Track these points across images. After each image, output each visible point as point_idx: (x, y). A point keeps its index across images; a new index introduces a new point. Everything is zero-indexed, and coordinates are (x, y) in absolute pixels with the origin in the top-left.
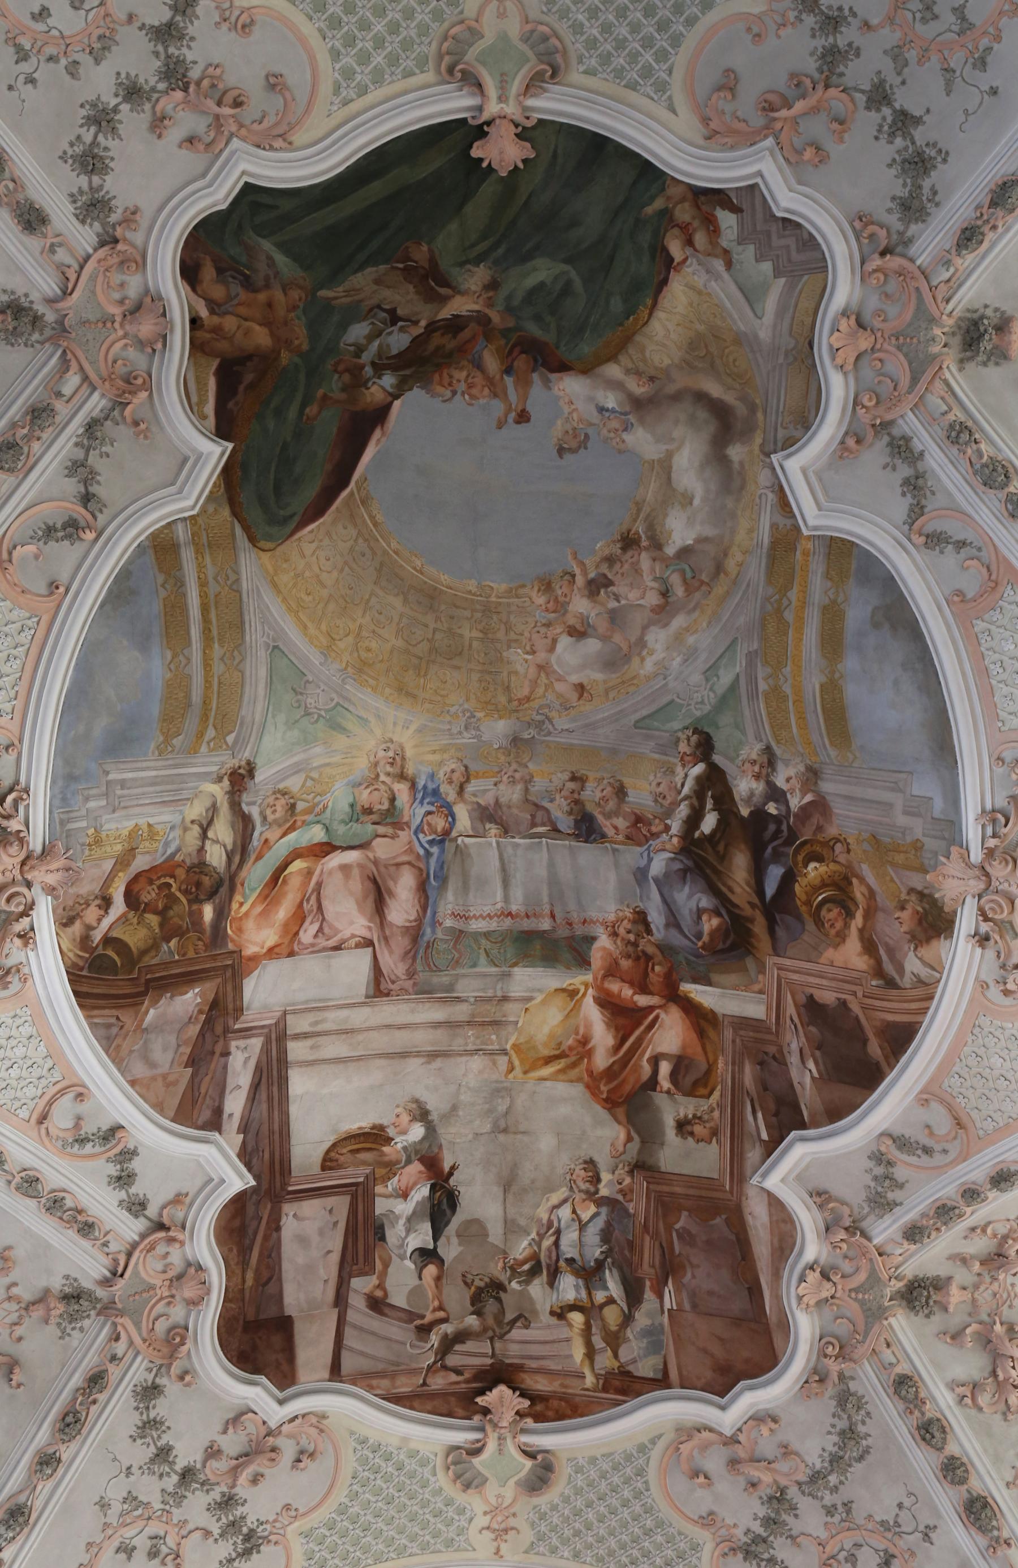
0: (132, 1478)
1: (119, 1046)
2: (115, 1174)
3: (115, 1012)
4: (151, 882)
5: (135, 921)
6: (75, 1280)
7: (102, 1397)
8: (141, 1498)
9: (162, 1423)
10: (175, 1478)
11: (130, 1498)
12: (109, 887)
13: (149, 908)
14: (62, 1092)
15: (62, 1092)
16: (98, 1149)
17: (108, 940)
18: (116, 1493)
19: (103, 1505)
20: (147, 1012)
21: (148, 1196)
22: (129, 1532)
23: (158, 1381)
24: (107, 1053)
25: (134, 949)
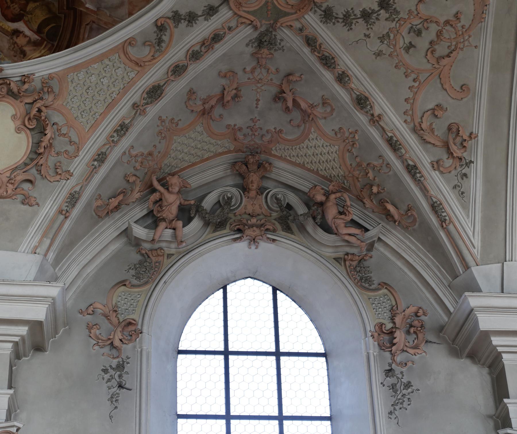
0: (372, 35)
1: (105, 23)
2: (187, 22)
3: (83, 27)
4: (8, 7)
5: (29, 16)
6: (250, 41)
7: (320, 40)
8: (385, 32)
9: (348, 12)
10: (382, 12)
11: (382, 39)
12: (7, 31)
13: (23, 8)
14: (126, 53)
15: (126, 53)
16: (168, 33)
17: (38, 32)
18: (376, 45)
19: (379, 54)
20: (87, 8)
21: (207, 4)
22: (401, 43)
23: (323, 9)
24: (107, 29)
25: (47, 17)
